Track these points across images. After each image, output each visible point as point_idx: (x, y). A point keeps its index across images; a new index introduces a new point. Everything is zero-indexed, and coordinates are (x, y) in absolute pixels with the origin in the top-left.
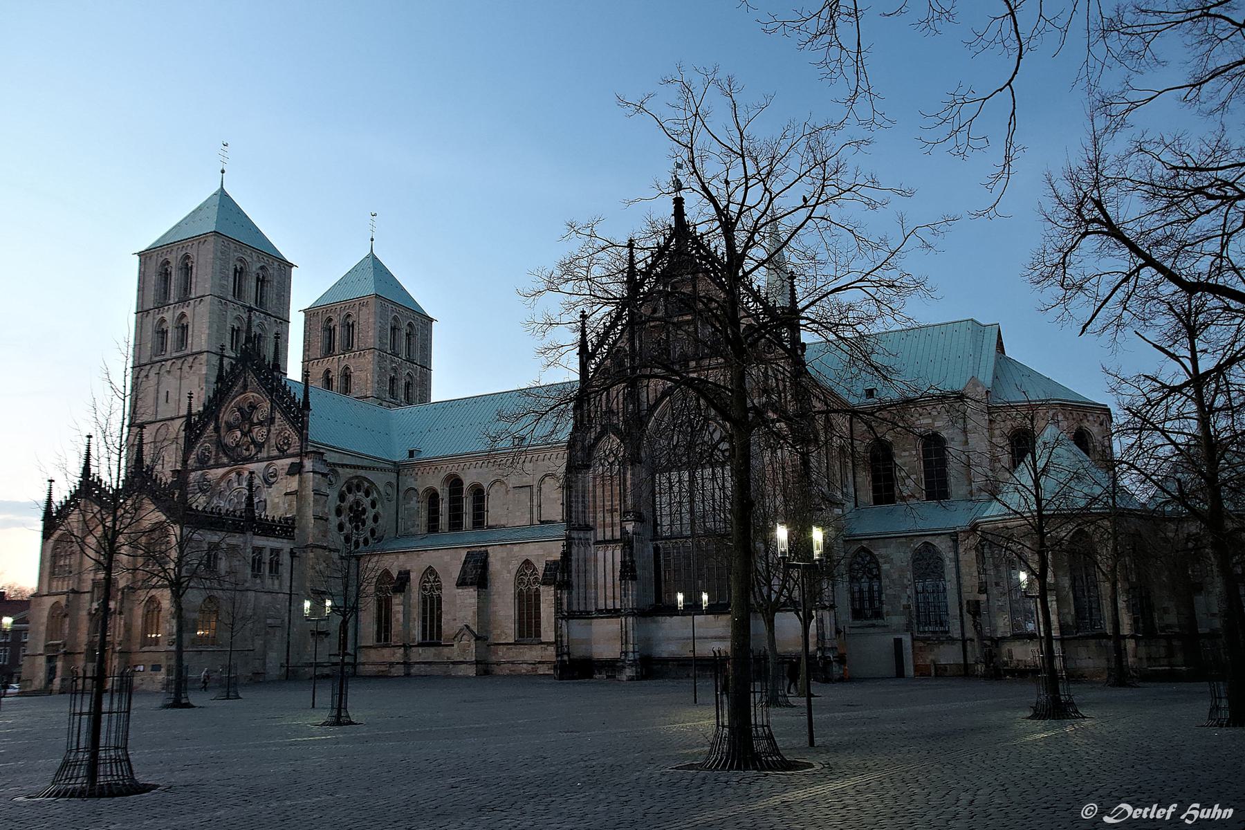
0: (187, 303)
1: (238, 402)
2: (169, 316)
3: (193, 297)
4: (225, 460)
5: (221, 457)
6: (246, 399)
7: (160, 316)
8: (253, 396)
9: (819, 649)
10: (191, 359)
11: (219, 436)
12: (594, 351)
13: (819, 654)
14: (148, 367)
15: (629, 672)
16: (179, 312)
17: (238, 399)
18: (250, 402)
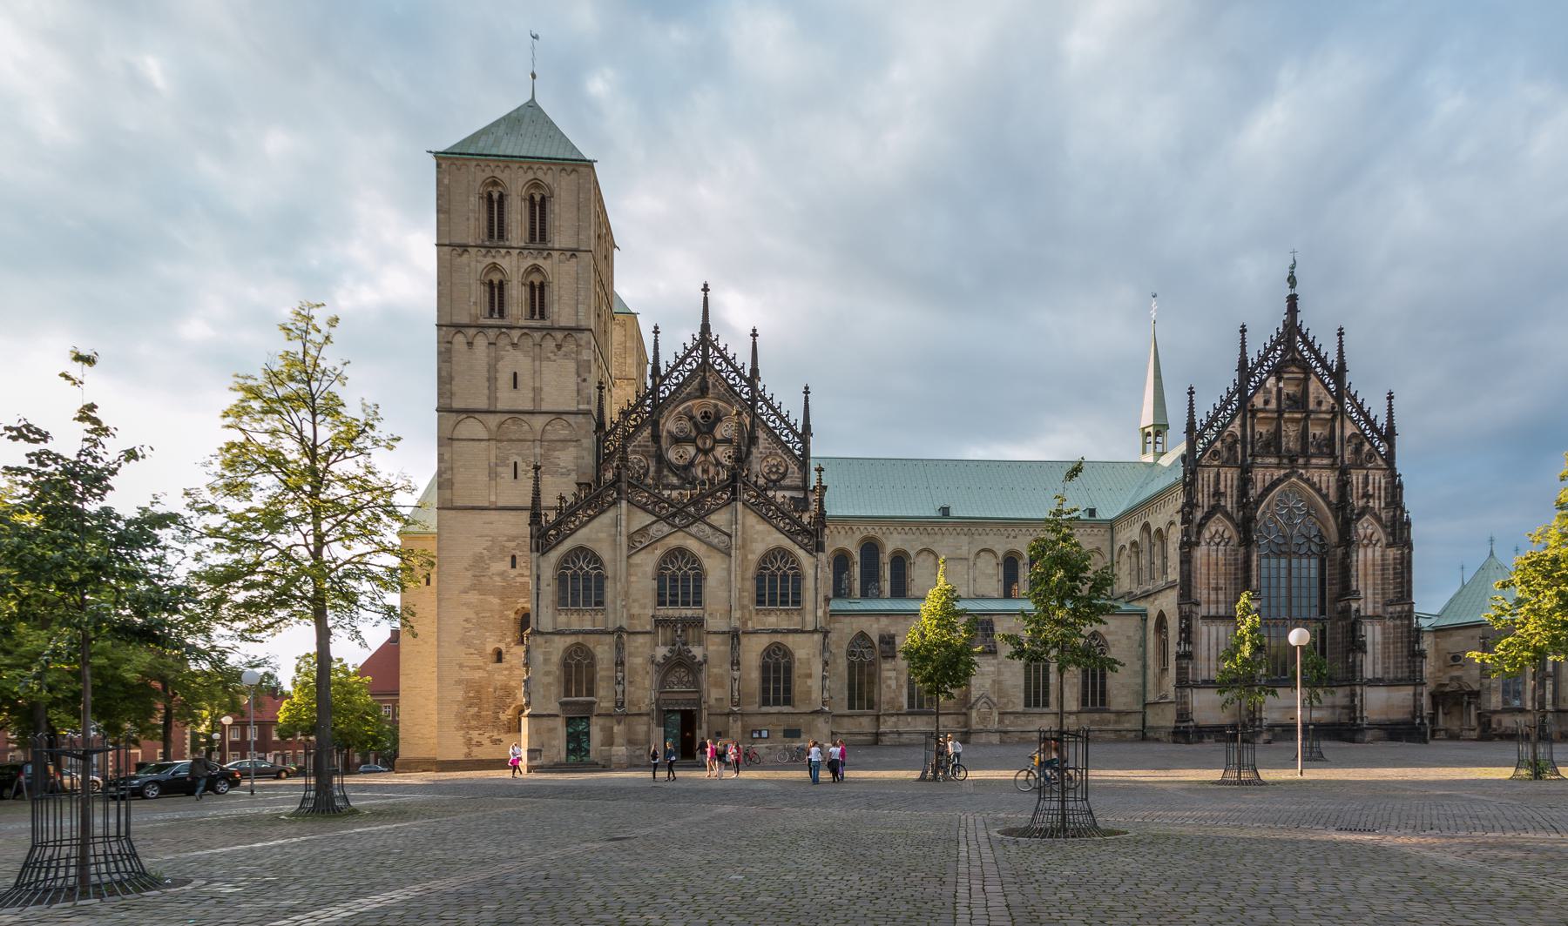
0: (545, 253)
1: (690, 409)
2: (513, 266)
3: (557, 246)
4: (675, 481)
5: (666, 476)
6: (701, 405)
8: (716, 406)
9: (1414, 718)
10: (559, 335)
11: (660, 448)
12: (1202, 431)
13: (1418, 721)
15: (1265, 736)
16: (530, 262)
17: (689, 403)
18: (706, 412)
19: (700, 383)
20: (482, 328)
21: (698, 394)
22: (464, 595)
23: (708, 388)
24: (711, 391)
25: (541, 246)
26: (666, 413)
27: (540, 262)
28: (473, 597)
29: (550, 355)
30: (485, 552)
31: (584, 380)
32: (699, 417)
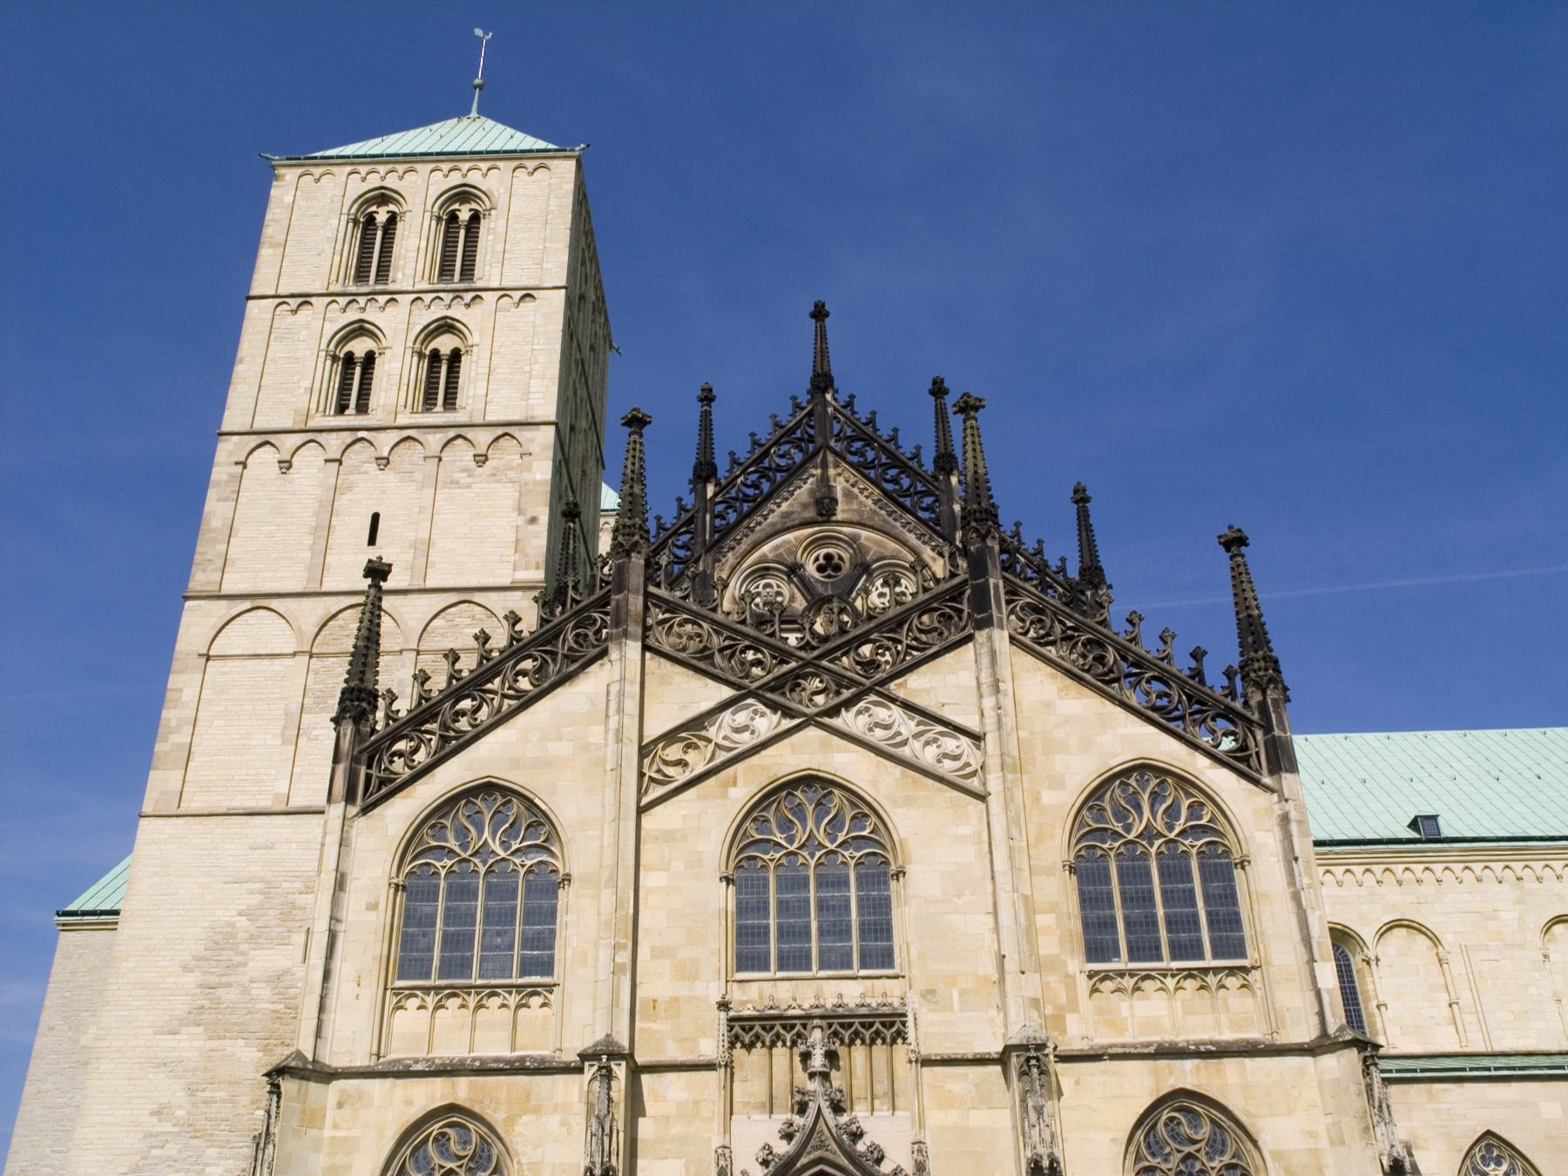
0: (468, 296)
3: (495, 284)
6: (817, 542)
7: (353, 315)
8: (854, 539)
10: (483, 438)
14: (298, 439)
16: (437, 312)
17: (790, 536)
18: (828, 557)
19: (812, 492)
20: (312, 434)
21: (810, 514)
22: (168, 1041)
23: (835, 501)
24: (840, 507)
25: (462, 286)
26: (731, 558)
27: (458, 312)
28: (190, 1044)
29: (457, 476)
30: (242, 922)
31: (533, 520)
32: (811, 569)
